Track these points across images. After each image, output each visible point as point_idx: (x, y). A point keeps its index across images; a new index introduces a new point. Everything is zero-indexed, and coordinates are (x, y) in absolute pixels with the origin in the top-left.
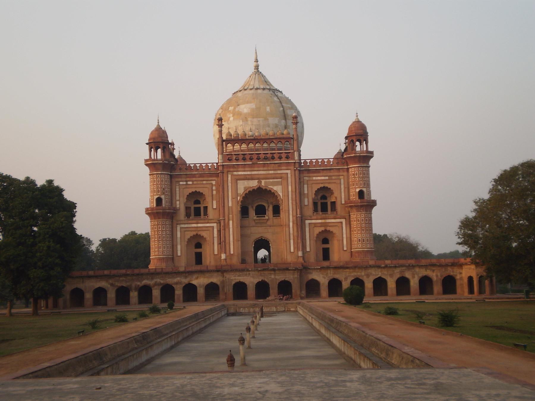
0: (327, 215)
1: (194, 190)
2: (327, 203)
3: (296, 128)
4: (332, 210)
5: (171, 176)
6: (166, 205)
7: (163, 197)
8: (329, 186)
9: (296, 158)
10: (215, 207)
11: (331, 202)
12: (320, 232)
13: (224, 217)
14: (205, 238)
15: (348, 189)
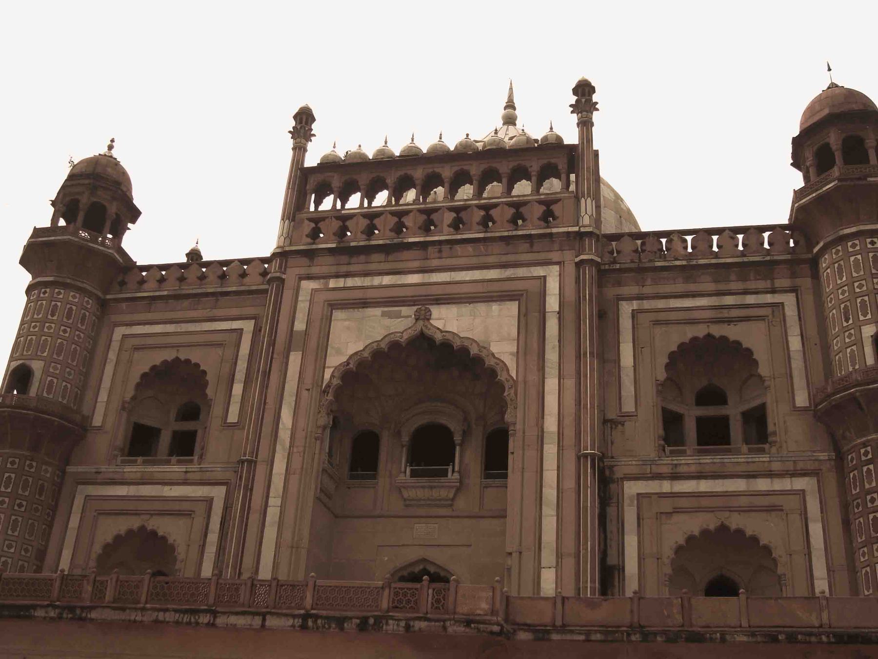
0: (728, 459)
1: (169, 355)
2: (725, 420)
3: (586, 125)
4: (747, 441)
5: (103, 305)
6: (39, 398)
7: (37, 366)
8: (732, 332)
9: (586, 220)
10: (233, 418)
11: (745, 414)
12: (690, 539)
13: (256, 451)
14: (172, 548)
15: (820, 342)
